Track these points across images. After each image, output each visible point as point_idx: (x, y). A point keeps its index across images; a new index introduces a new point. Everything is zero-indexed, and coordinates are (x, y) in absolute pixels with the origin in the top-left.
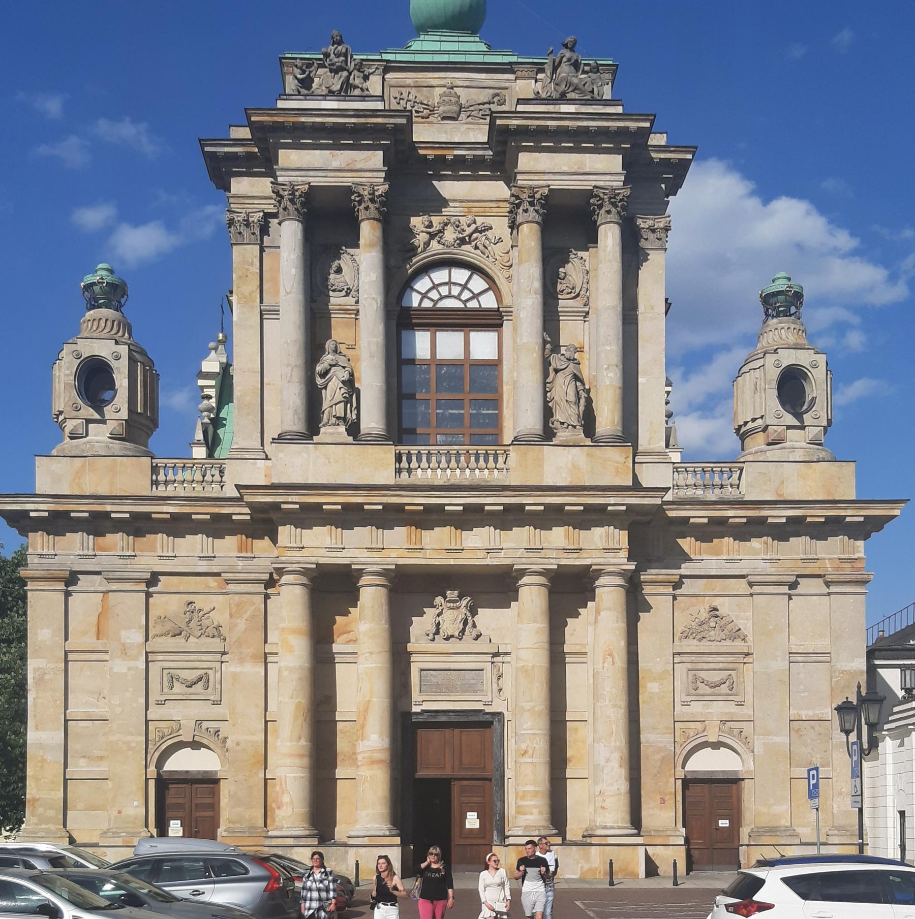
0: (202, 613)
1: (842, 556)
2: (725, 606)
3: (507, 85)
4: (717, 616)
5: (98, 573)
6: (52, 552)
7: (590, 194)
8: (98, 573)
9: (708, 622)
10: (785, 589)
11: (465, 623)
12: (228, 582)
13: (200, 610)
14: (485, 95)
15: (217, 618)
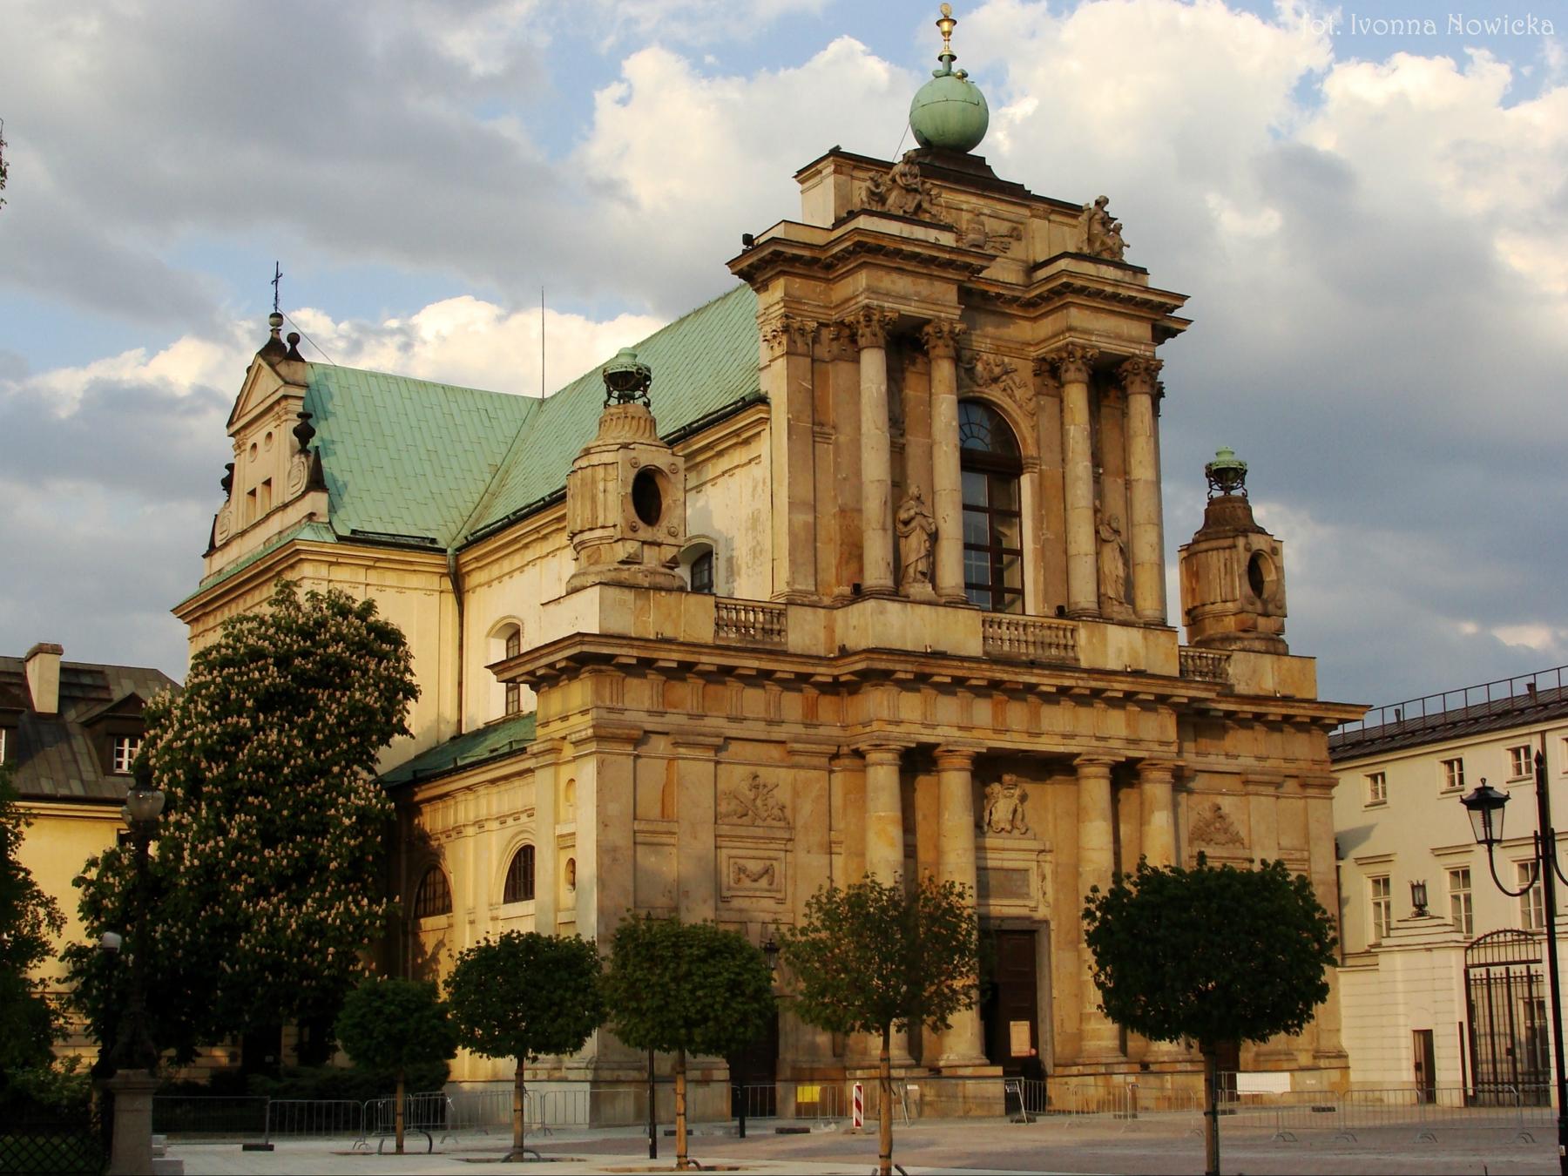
0: (766, 790)
1: (1316, 758)
2: (1227, 804)
3: (1024, 220)
4: (1221, 817)
5: (667, 734)
6: (620, 705)
7: (1124, 359)
8: (667, 734)
9: (1213, 823)
10: (1271, 790)
11: (1015, 811)
12: (792, 753)
13: (765, 786)
14: (1004, 228)
15: (783, 795)
